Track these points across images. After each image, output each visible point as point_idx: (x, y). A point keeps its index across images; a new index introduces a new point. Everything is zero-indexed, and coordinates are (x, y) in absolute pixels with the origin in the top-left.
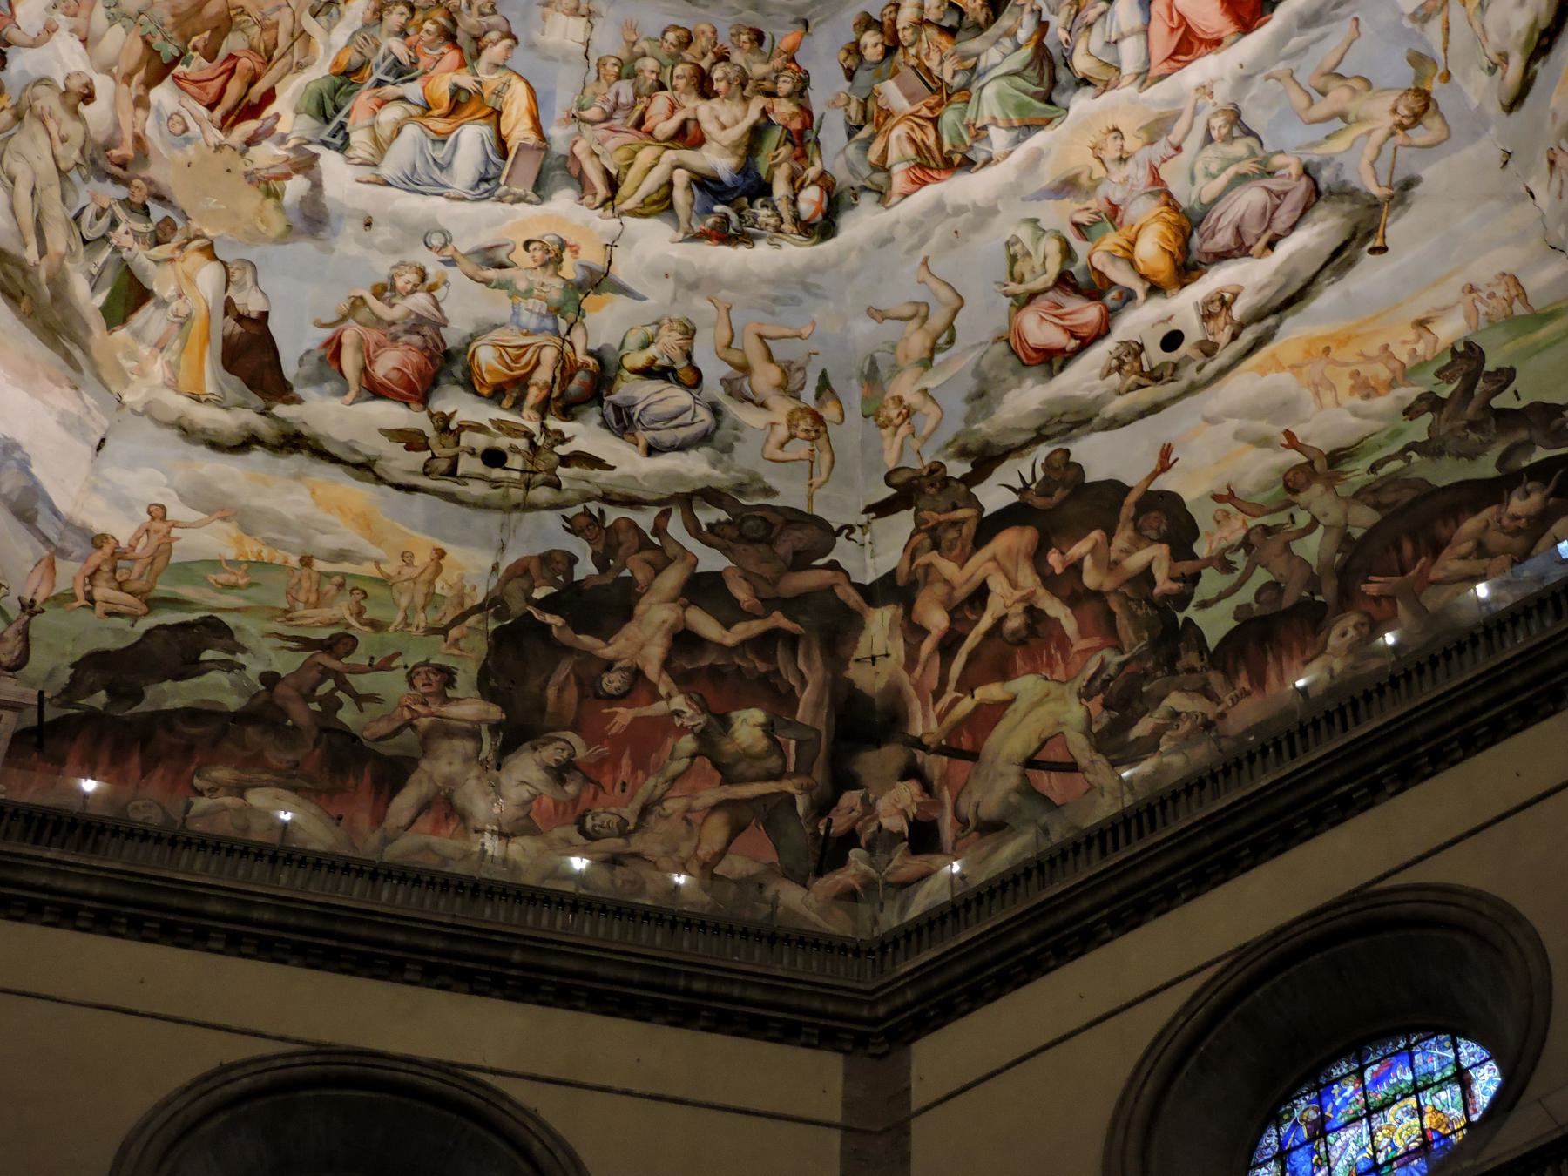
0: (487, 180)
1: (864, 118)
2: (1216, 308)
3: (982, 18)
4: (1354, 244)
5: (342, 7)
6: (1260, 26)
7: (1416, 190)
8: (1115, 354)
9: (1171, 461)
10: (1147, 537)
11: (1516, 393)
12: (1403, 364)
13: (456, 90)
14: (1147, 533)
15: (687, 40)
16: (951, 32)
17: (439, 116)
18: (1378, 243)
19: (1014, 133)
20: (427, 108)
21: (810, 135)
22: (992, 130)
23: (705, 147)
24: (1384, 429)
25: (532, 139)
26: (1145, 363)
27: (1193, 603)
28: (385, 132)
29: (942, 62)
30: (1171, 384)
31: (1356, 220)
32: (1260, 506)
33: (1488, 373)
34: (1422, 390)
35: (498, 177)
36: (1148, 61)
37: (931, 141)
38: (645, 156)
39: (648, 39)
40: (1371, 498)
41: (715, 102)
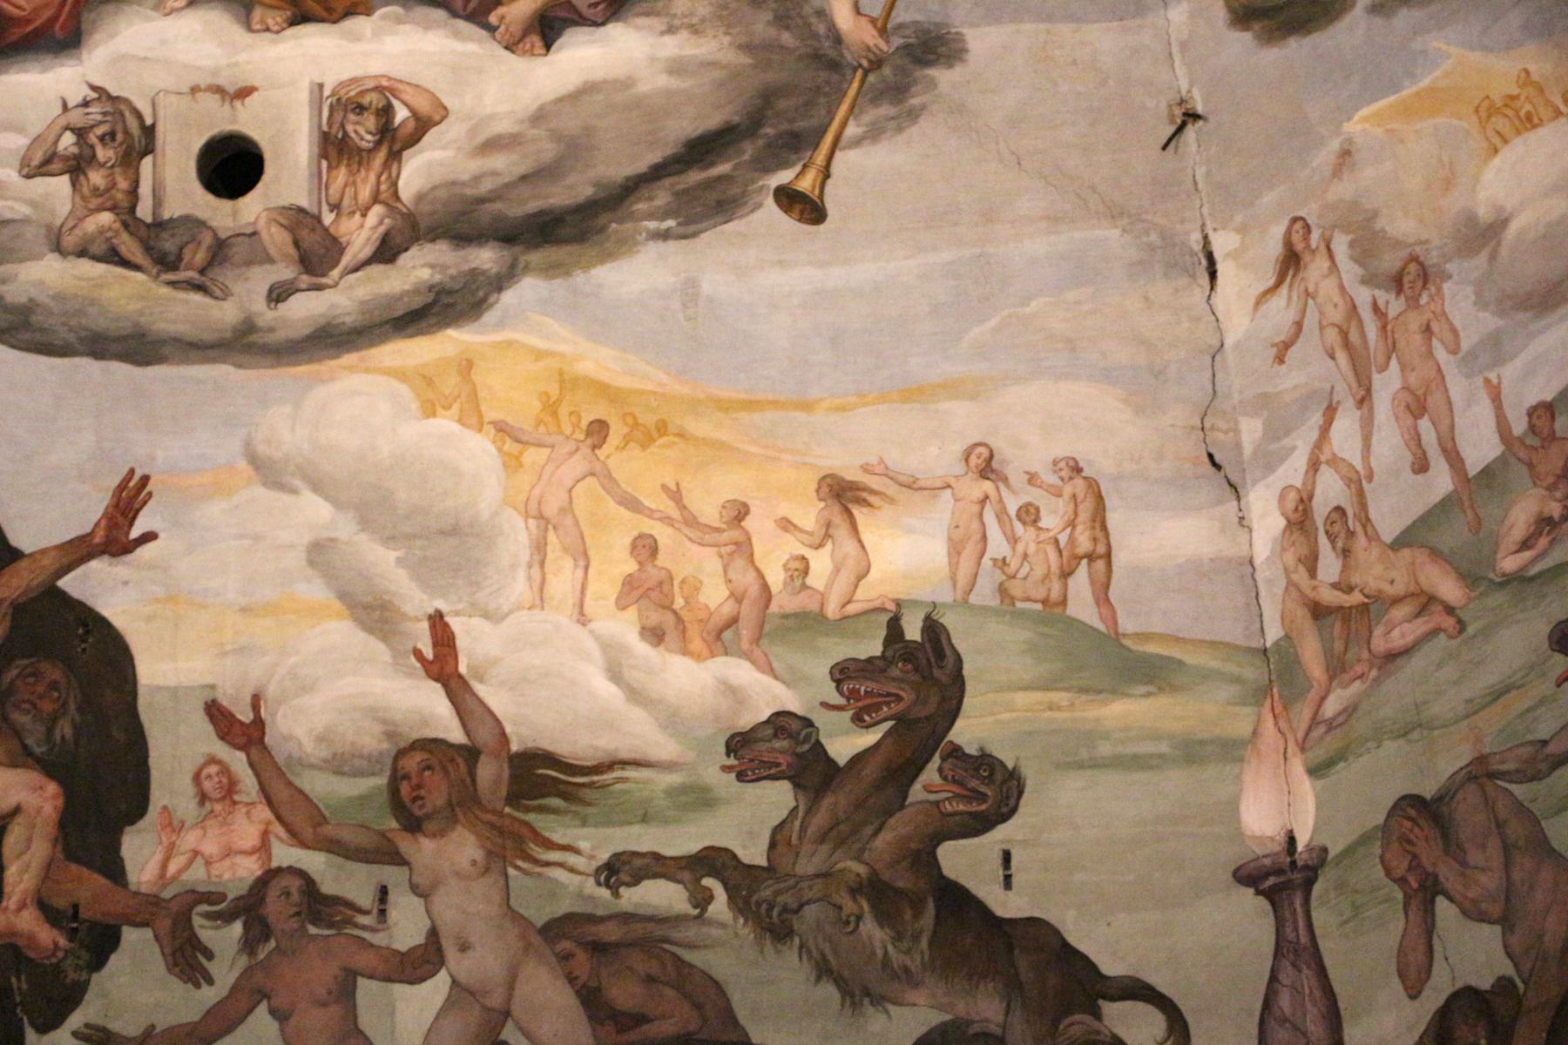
2: (362, 131)
4: (749, 150)
7: (944, 77)
8: (76, 118)
9: (135, 533)
10: (17, 733)
11: (1007, 857)
12: (765, 587)
14: (22, 719)
18: (806, 184)
24: (669, 766)
26: (145, 189)
27: (76, 1020)
30: (196, 297)
31: (771, 77)
32: (319, 819)
33: (956, 752)
34: (791, 701)
40: (583, 963)
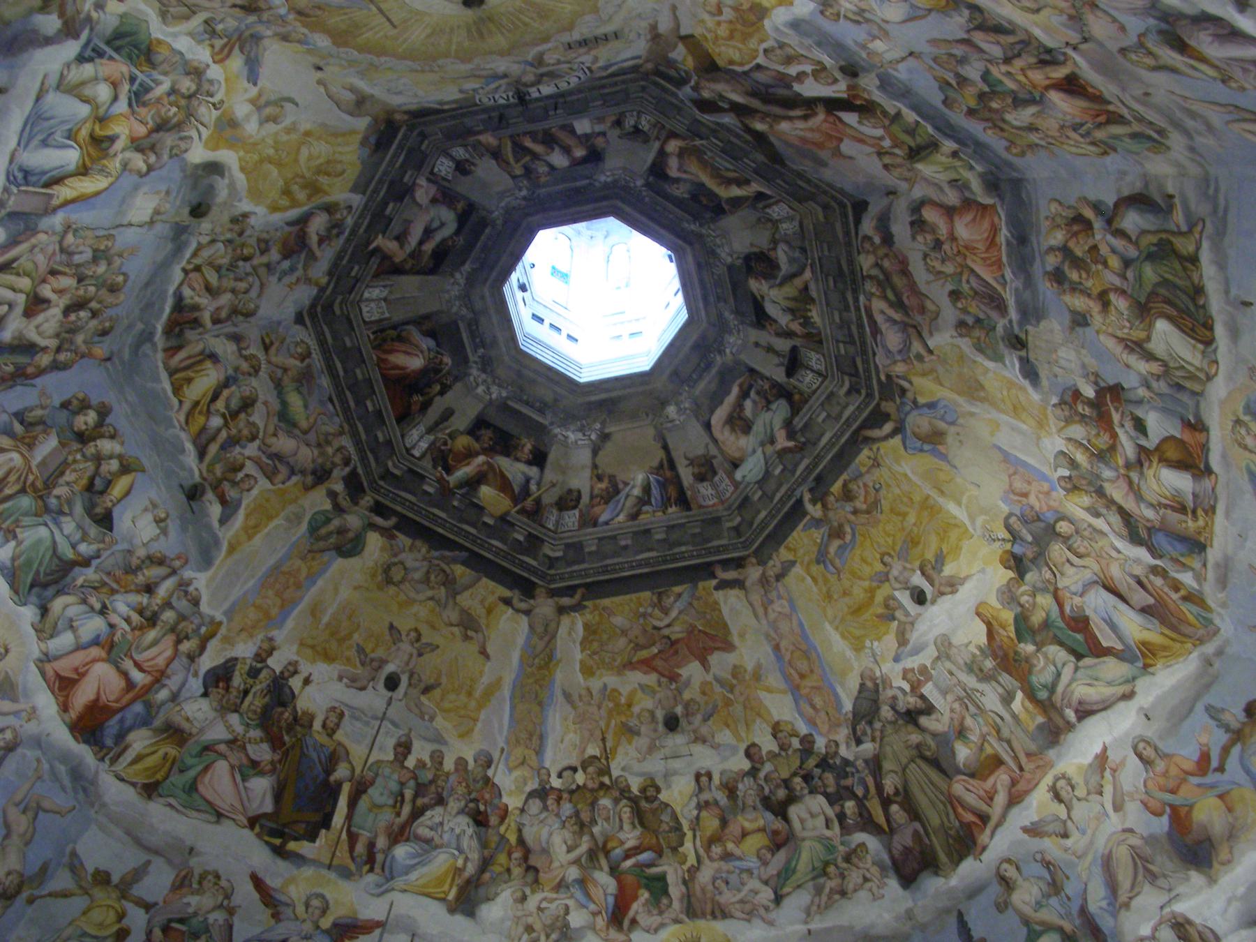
0: (25, 178)
1: (31, 424)
3: (99, 510)
5: (208, 42)
6: (74, 737)
13: (112, 139)
15: (113, 289)
16: (90, 487)
17: (93, 130)
19: (8, 563)
20: (102, 120)
21: (19, 381)
22: (13, 544)
23: (24, 319)
25: (55, 202)
28: (87, 91)
29: (68, 483)
35: (27, 184)
36: (57, 658)
37: (8, 491)
38: (25, 283)
39: (122, 264)
41: (60, 316)
